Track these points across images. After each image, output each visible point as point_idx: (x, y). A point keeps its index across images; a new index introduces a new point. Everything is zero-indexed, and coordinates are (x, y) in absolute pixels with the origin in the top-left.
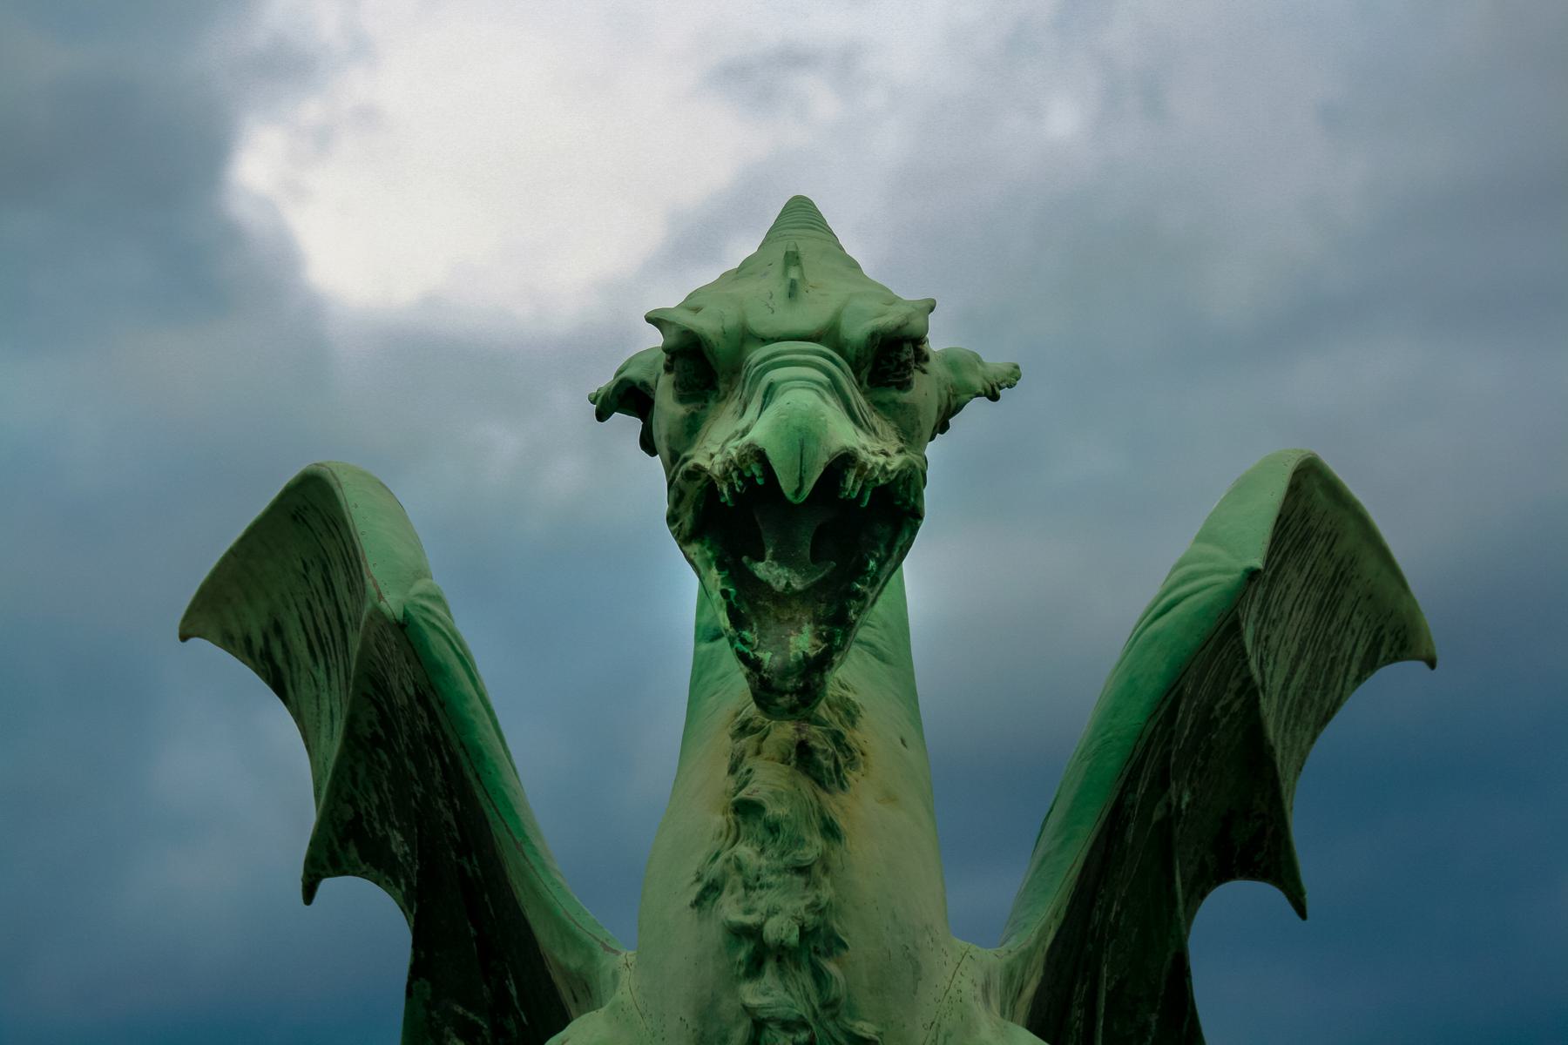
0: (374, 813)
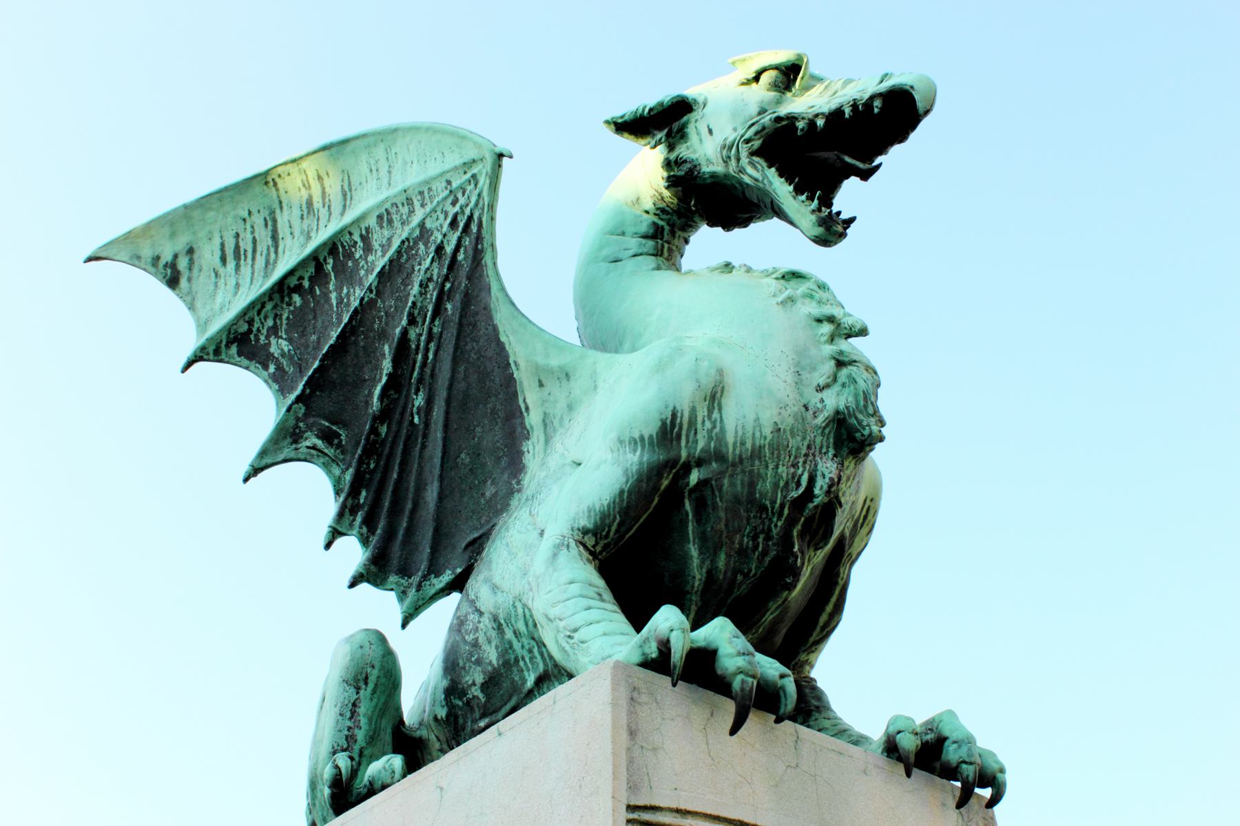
0: (264, 331)
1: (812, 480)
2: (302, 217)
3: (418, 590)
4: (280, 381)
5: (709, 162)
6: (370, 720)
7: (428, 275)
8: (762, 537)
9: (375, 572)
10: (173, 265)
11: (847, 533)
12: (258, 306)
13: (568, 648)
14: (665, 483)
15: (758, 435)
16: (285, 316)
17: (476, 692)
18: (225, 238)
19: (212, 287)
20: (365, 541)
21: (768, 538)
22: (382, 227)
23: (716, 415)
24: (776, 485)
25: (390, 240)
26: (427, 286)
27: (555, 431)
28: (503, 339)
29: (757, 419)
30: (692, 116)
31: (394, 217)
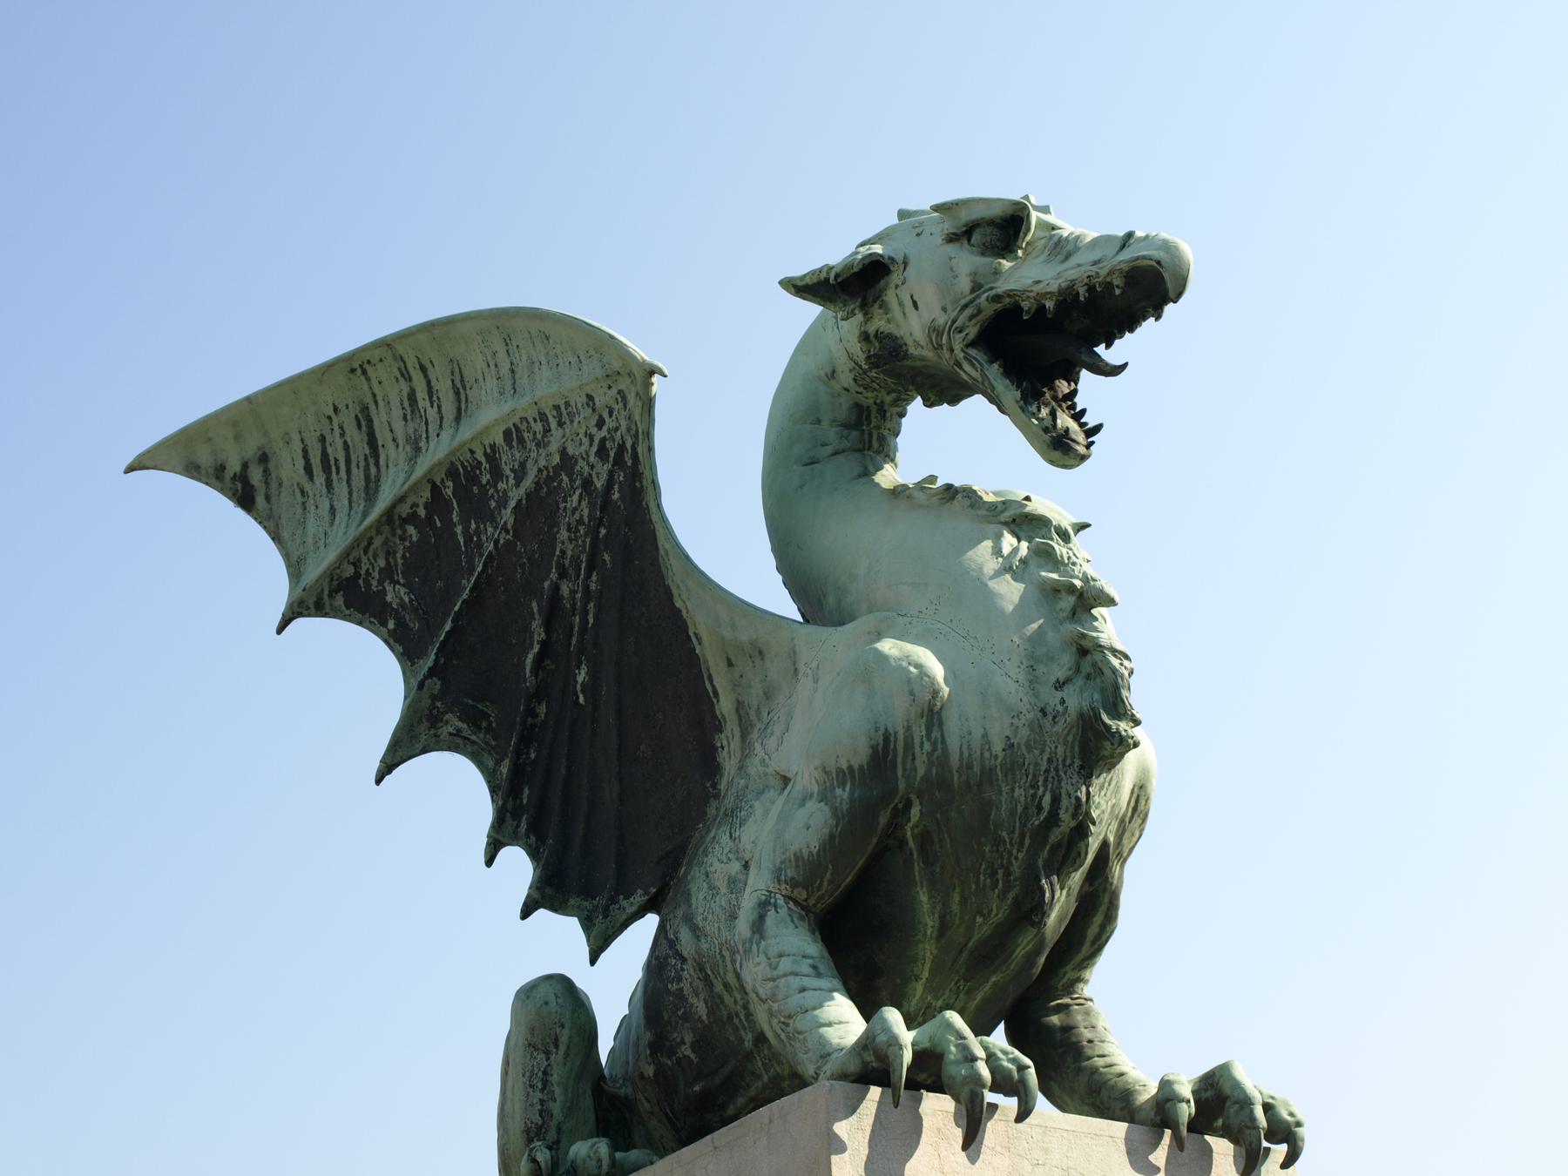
0: (376, 575)
1: (1056, 801)
2: (405, 417)
3: (605, 917)
4: (406, 645)
5: (917, 344)
6: (566, 1089)
7: (577, 516)
8: (1000, 872)
9: (548, 893)
10: (243, 477)
11: (1111, 839)
12: (363, 543)
13: (783, 1036)
14: (883, 819)
15: (987, 754)
16: (399, 556)
17: (686, 1050)
18: (308, 442)
19: (299, 510)
20: (534, 854)
21: (1008, 873)
22: (511, 447)
23: (935, 734)
24: (1012, 812)
25: (523, 465)
26: (577, 530)
27: (752, 726)
28: (678, 604)
29: (985, 735)
30: (895, 278)
31: (526, 435)
